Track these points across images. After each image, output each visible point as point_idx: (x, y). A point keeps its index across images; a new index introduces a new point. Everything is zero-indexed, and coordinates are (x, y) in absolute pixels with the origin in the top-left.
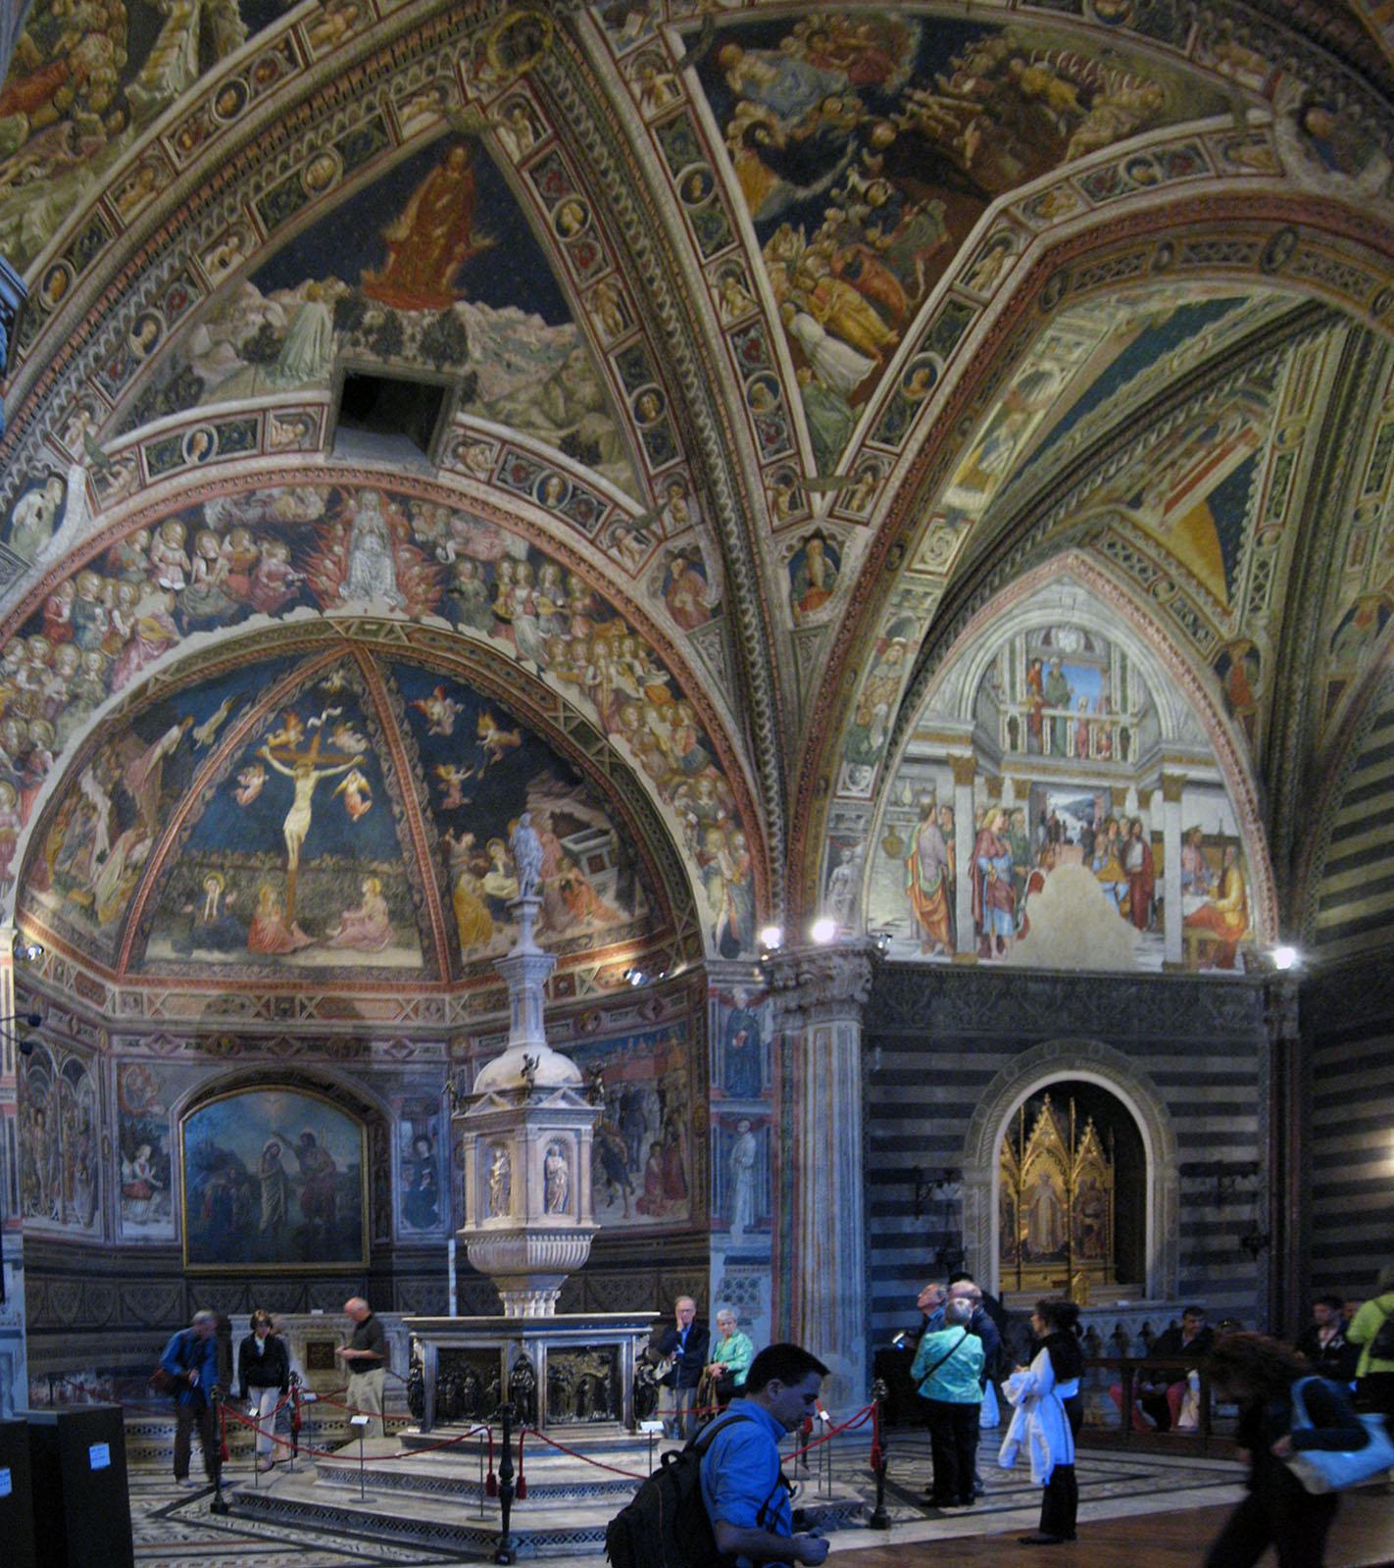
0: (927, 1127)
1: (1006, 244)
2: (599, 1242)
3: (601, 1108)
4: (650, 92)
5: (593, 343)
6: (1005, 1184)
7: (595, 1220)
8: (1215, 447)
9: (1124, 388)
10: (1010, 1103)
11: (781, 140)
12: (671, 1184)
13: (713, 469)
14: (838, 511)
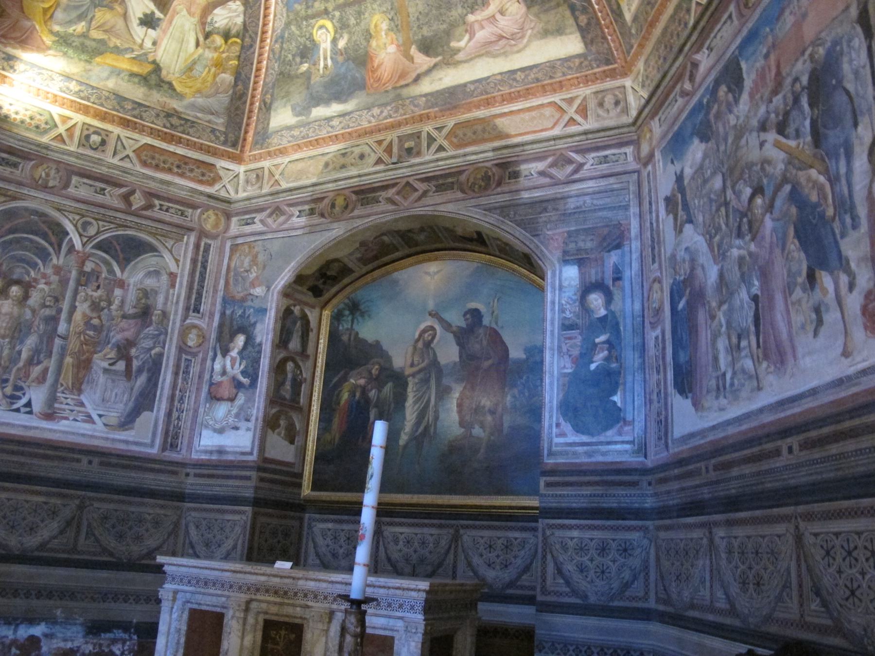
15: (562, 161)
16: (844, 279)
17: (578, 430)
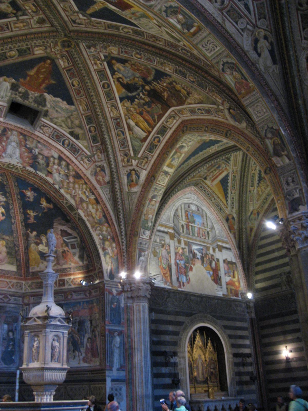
0: (167, 338)
1: (174, 117)
2: (70, 372)
3: (71, 325)
4: (96, 64)
5: (79, 112)
6: (189, 357)
7: (68, 366)
8: (220, 170)
9: (201, 153)
10: (189, 332)
11: (125, 82)
12: (93, 352)
13: (108, 148)
14: (139, 165)
15: (6, 297)
16: (80, 354)
17: (5, 364)
